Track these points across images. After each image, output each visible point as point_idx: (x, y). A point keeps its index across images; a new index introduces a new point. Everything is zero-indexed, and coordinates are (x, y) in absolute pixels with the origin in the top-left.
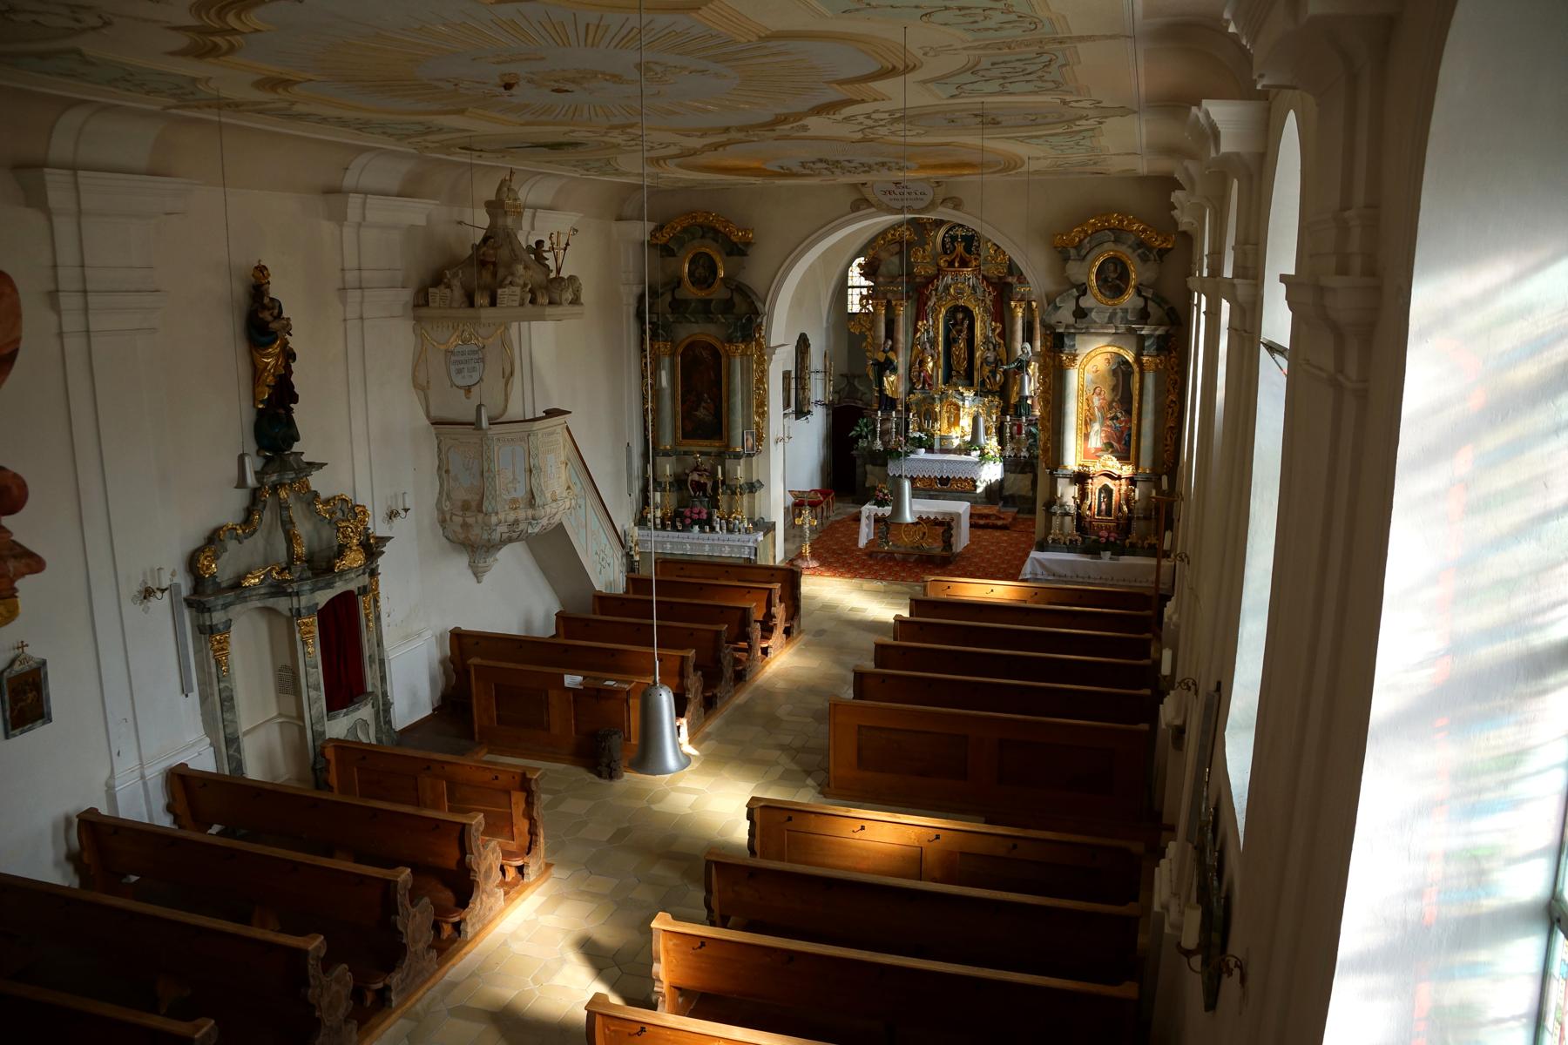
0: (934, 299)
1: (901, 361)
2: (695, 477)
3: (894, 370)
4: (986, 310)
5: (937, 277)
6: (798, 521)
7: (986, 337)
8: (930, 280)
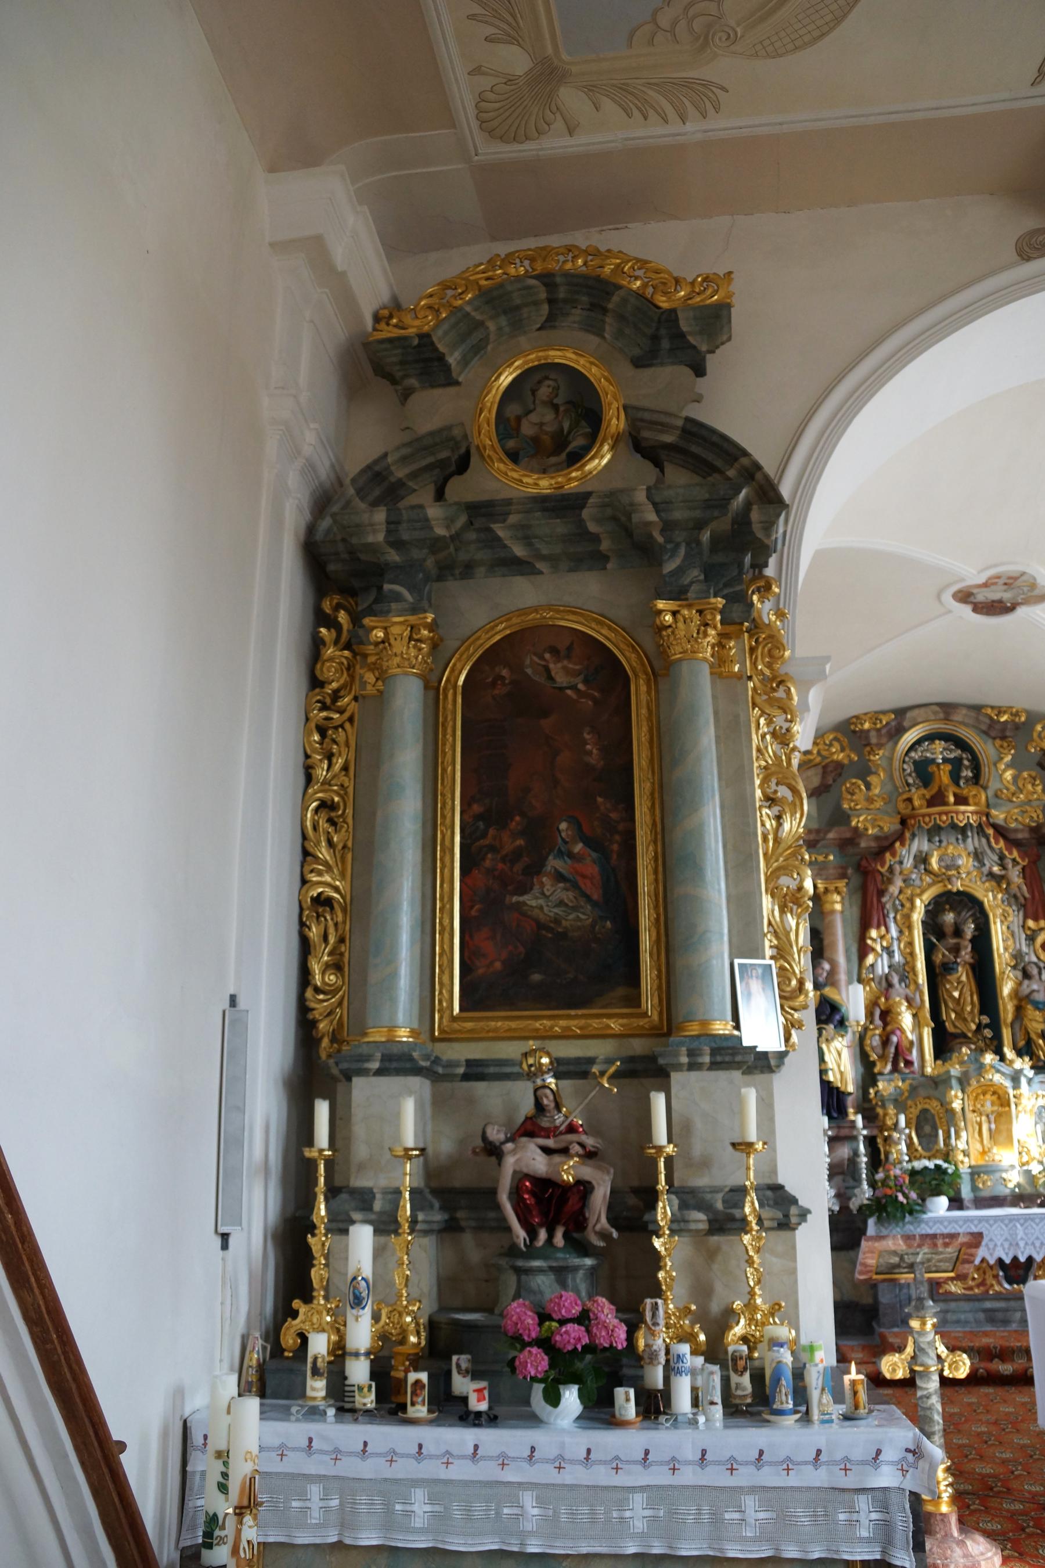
0: (899, 883)
2: (530, 1158)
4: (1013, 898)
5: (900, 837)
6: (894, 1366)
7: (1018, 956)
8: (886, 845)
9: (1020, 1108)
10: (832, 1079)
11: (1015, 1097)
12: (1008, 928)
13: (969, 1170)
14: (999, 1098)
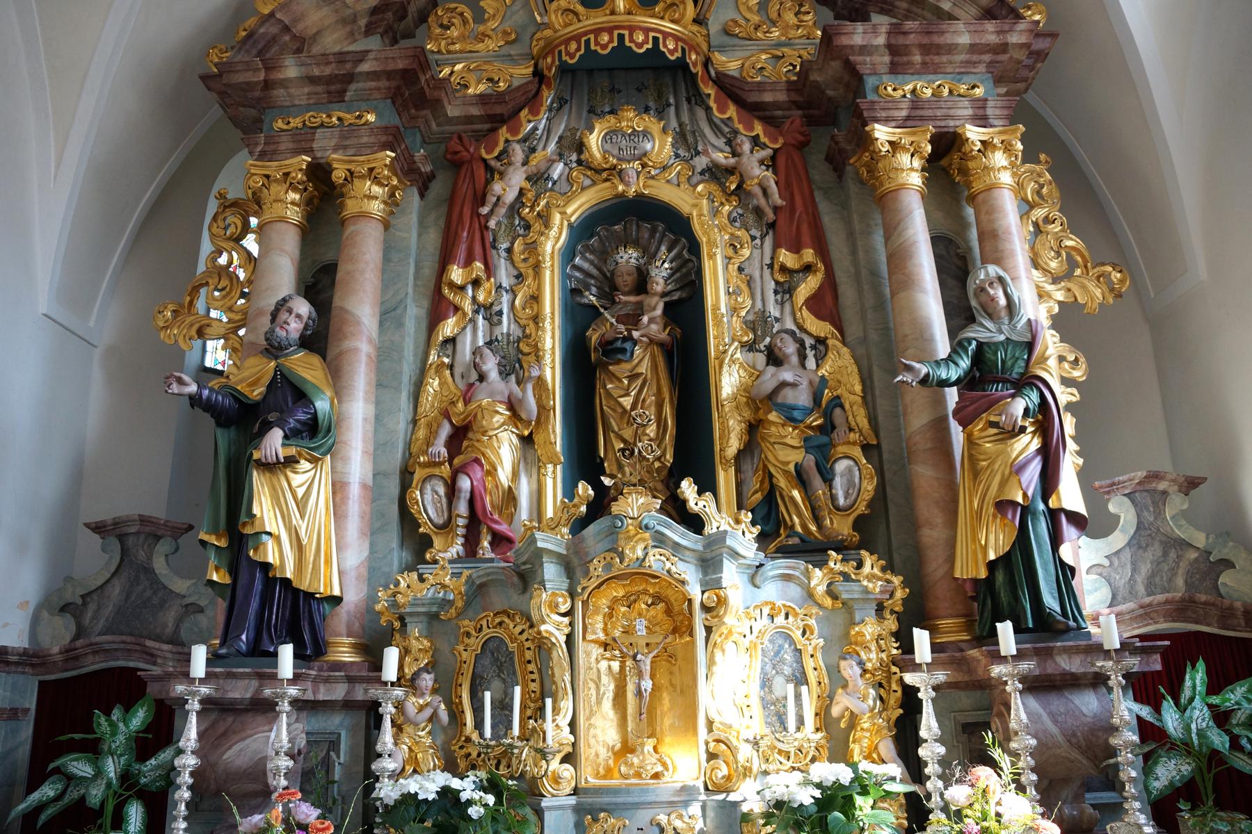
1: (358, 414)
3: (314, 434)
7: (758, 323)
9: (715, 637)
10: (271, 557)
11: (706, 609)
12: (740, 269)
13: (572, 801)
14: (669, 612)
